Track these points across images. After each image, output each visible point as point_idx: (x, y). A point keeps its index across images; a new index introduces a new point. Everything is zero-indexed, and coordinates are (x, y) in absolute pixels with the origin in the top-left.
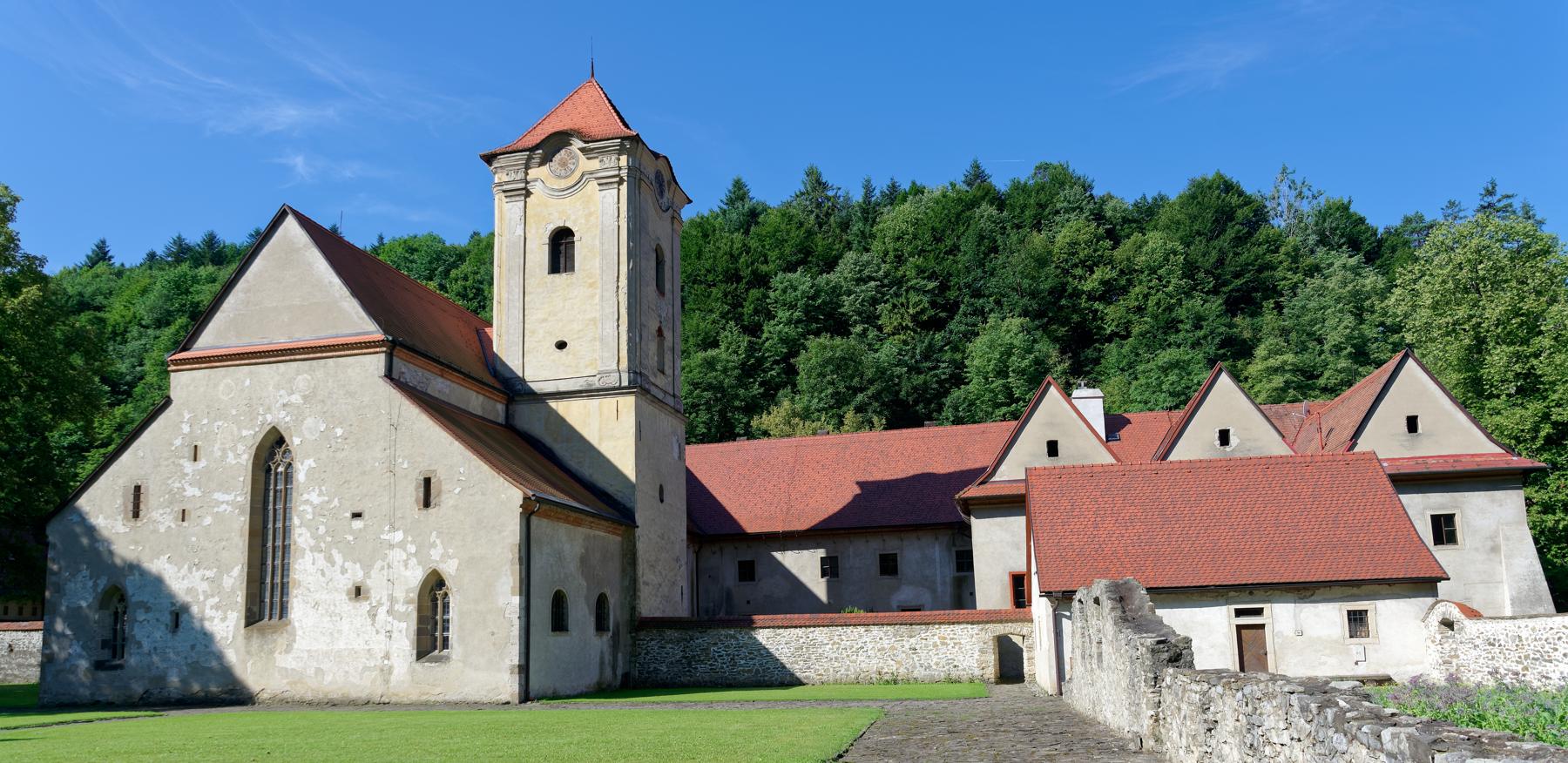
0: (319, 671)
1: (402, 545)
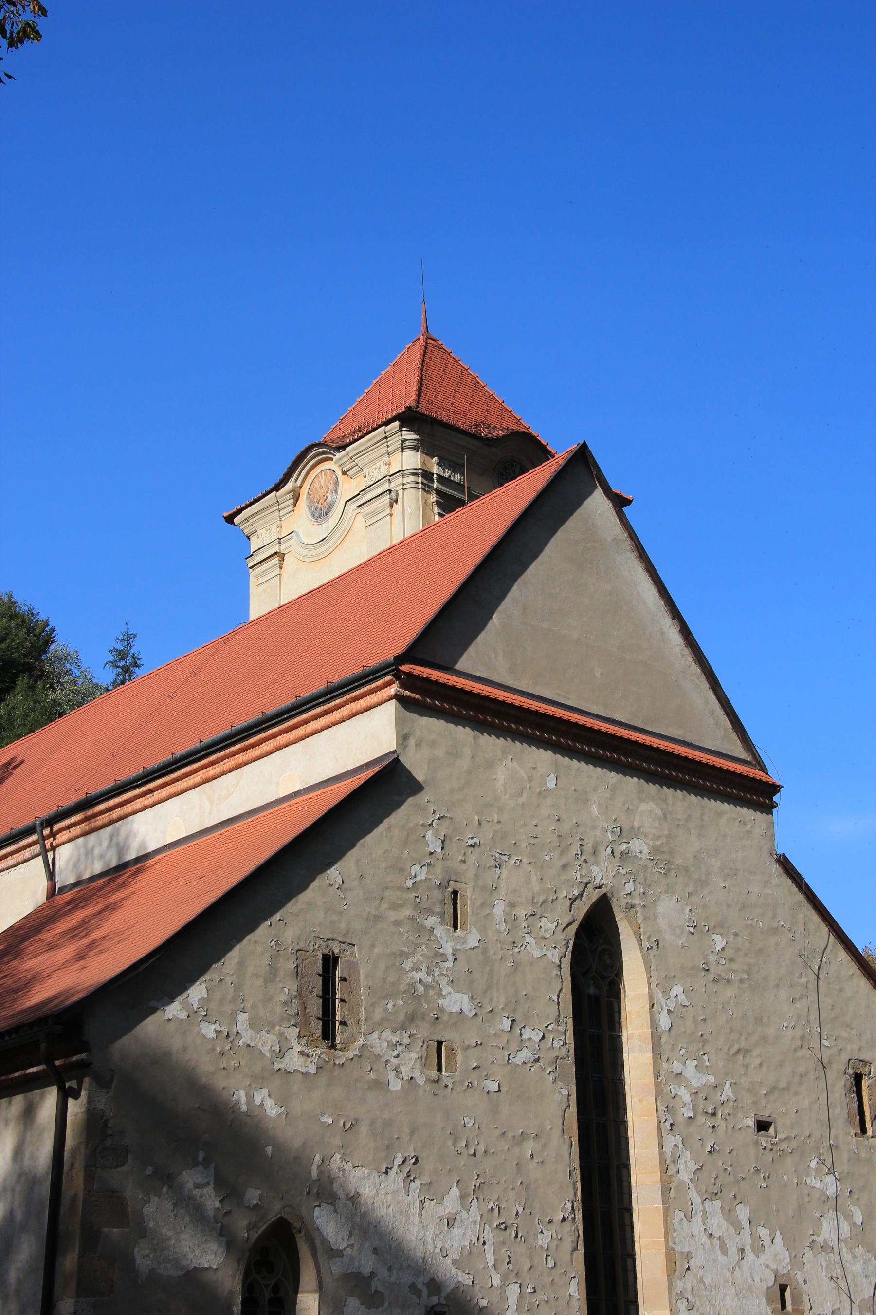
1: (836, 1204)
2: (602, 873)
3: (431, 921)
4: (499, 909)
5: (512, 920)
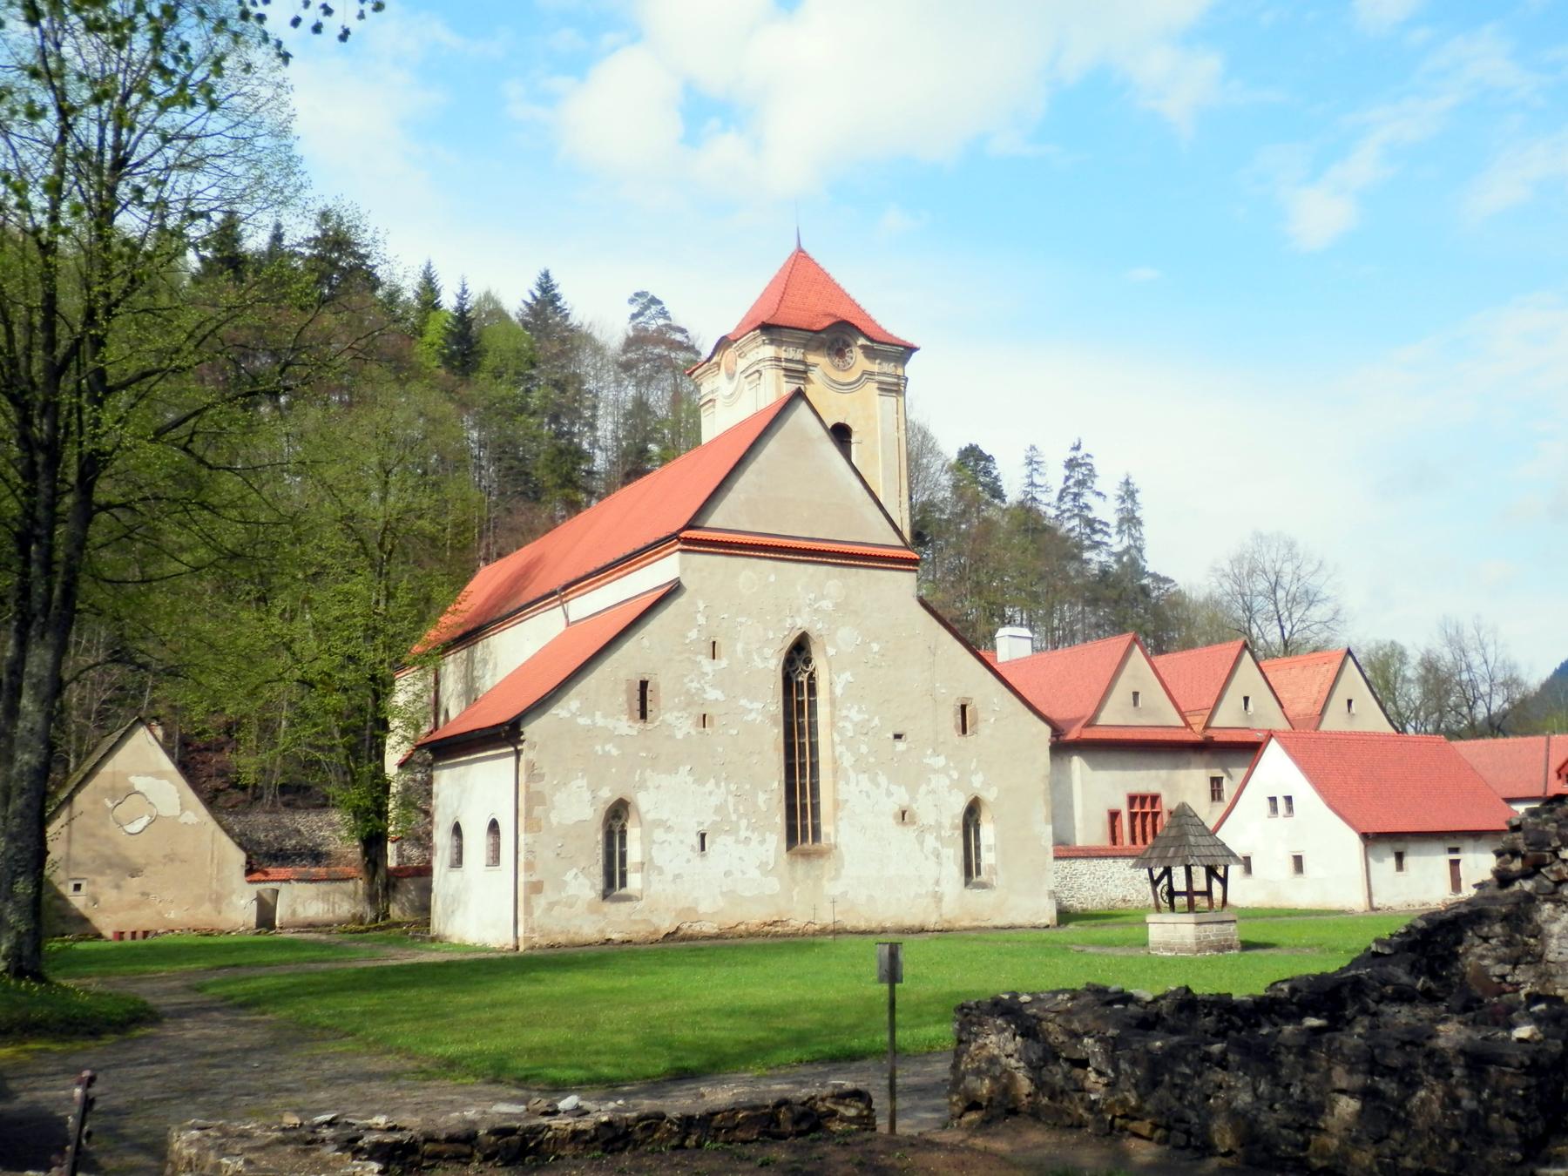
0: (871, 898)
2: (802, 623)
3: (700, 658)
4: (739, 646)
5: (747, 653)
